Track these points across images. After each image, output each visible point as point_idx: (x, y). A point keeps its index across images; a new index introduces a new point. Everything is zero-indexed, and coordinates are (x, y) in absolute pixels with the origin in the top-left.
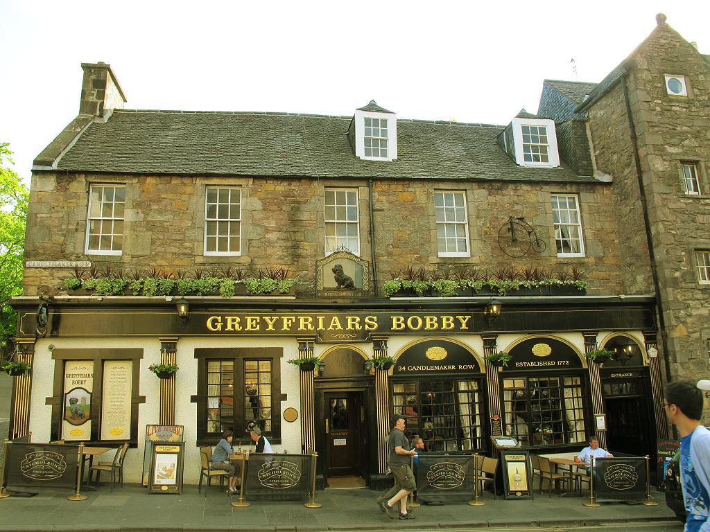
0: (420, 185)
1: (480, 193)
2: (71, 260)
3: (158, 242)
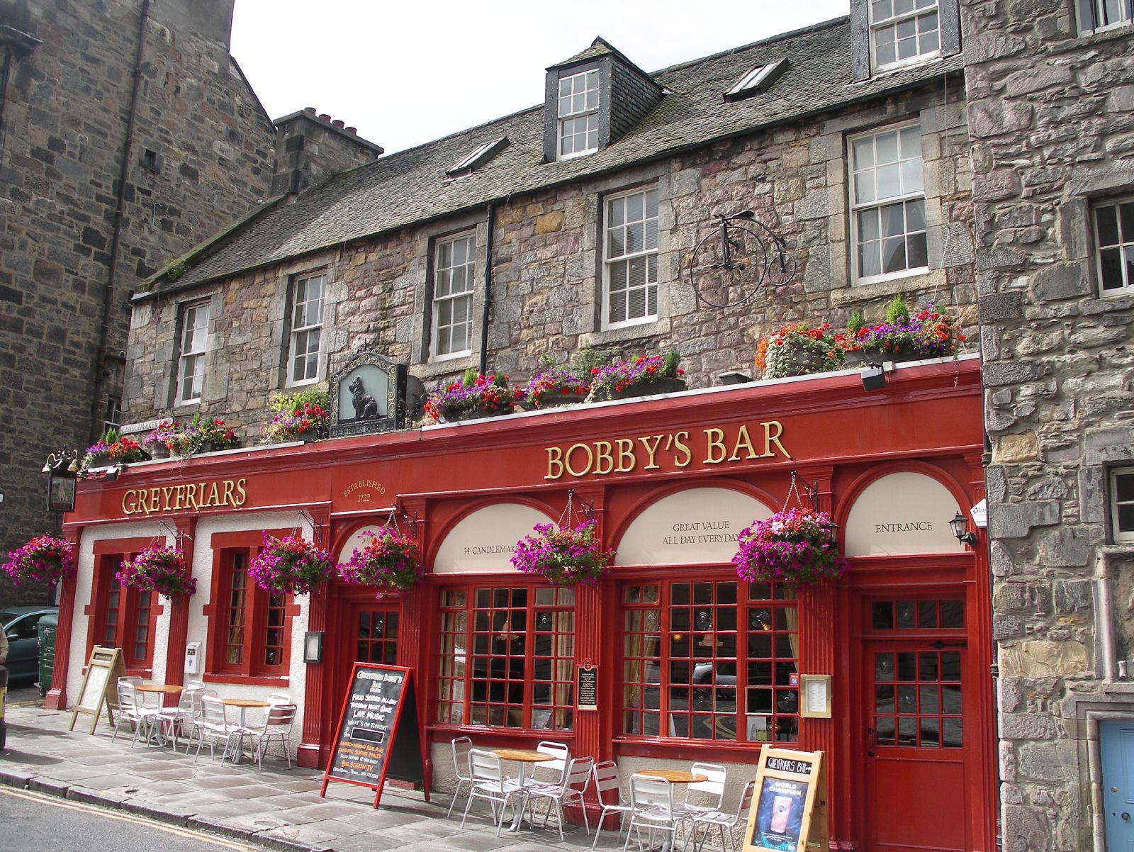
0: (573, 193)
1: (684, 178)
2: (158, 419)
3: (235, 376)
